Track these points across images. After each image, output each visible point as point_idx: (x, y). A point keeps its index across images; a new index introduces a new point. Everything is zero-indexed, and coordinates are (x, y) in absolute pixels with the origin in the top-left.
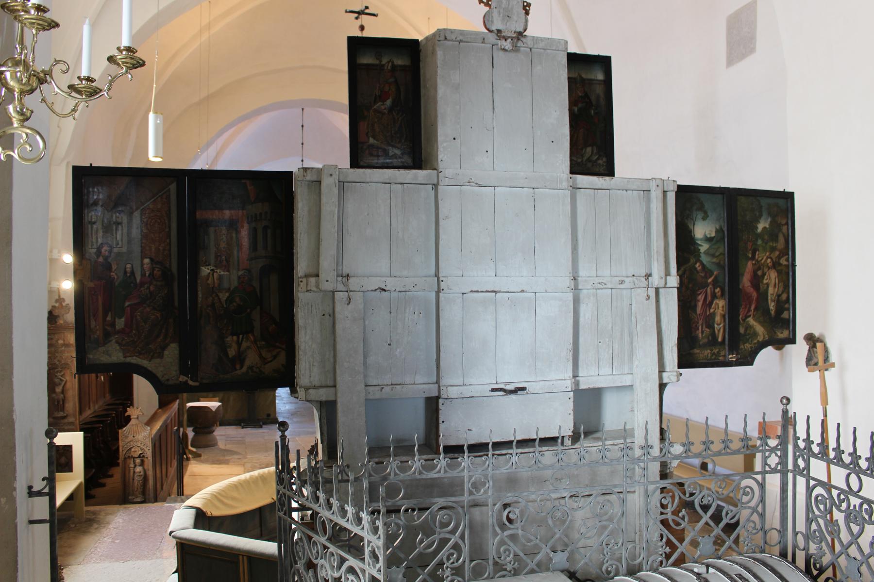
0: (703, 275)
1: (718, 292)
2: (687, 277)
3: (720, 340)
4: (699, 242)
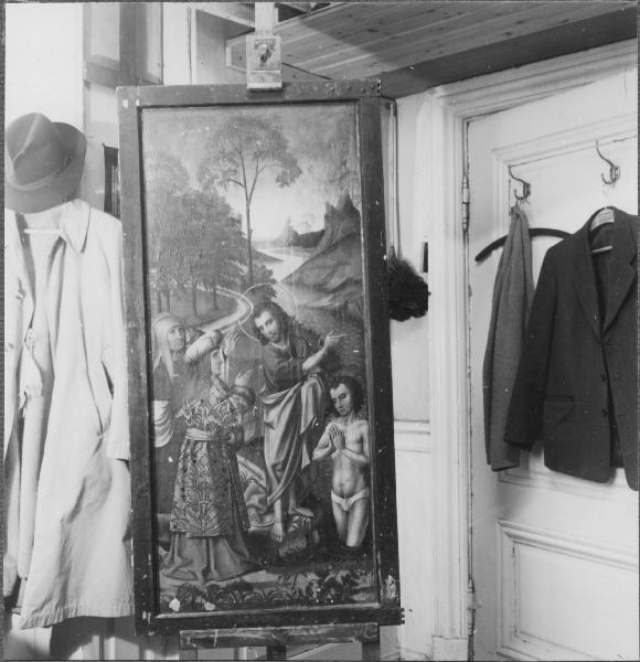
0: (283, 347)
1: (343, 396)
2: (225, 357)
4: (268, 252)
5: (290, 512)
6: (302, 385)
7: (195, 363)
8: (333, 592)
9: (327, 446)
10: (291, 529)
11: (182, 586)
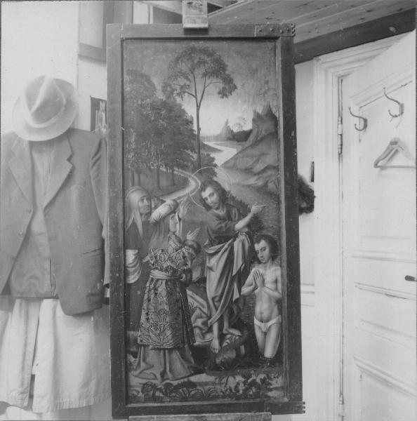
0: (222, 212)
1: (263, 249)
2: (180, 219)
3: (269, 353)
4: (211, 144)
5: (224, 332)
6: (234, 240)
7: (158, 223)
8: (254, 390)
9: (252, 285)
10: (225, 344)
11: (144, 384)
